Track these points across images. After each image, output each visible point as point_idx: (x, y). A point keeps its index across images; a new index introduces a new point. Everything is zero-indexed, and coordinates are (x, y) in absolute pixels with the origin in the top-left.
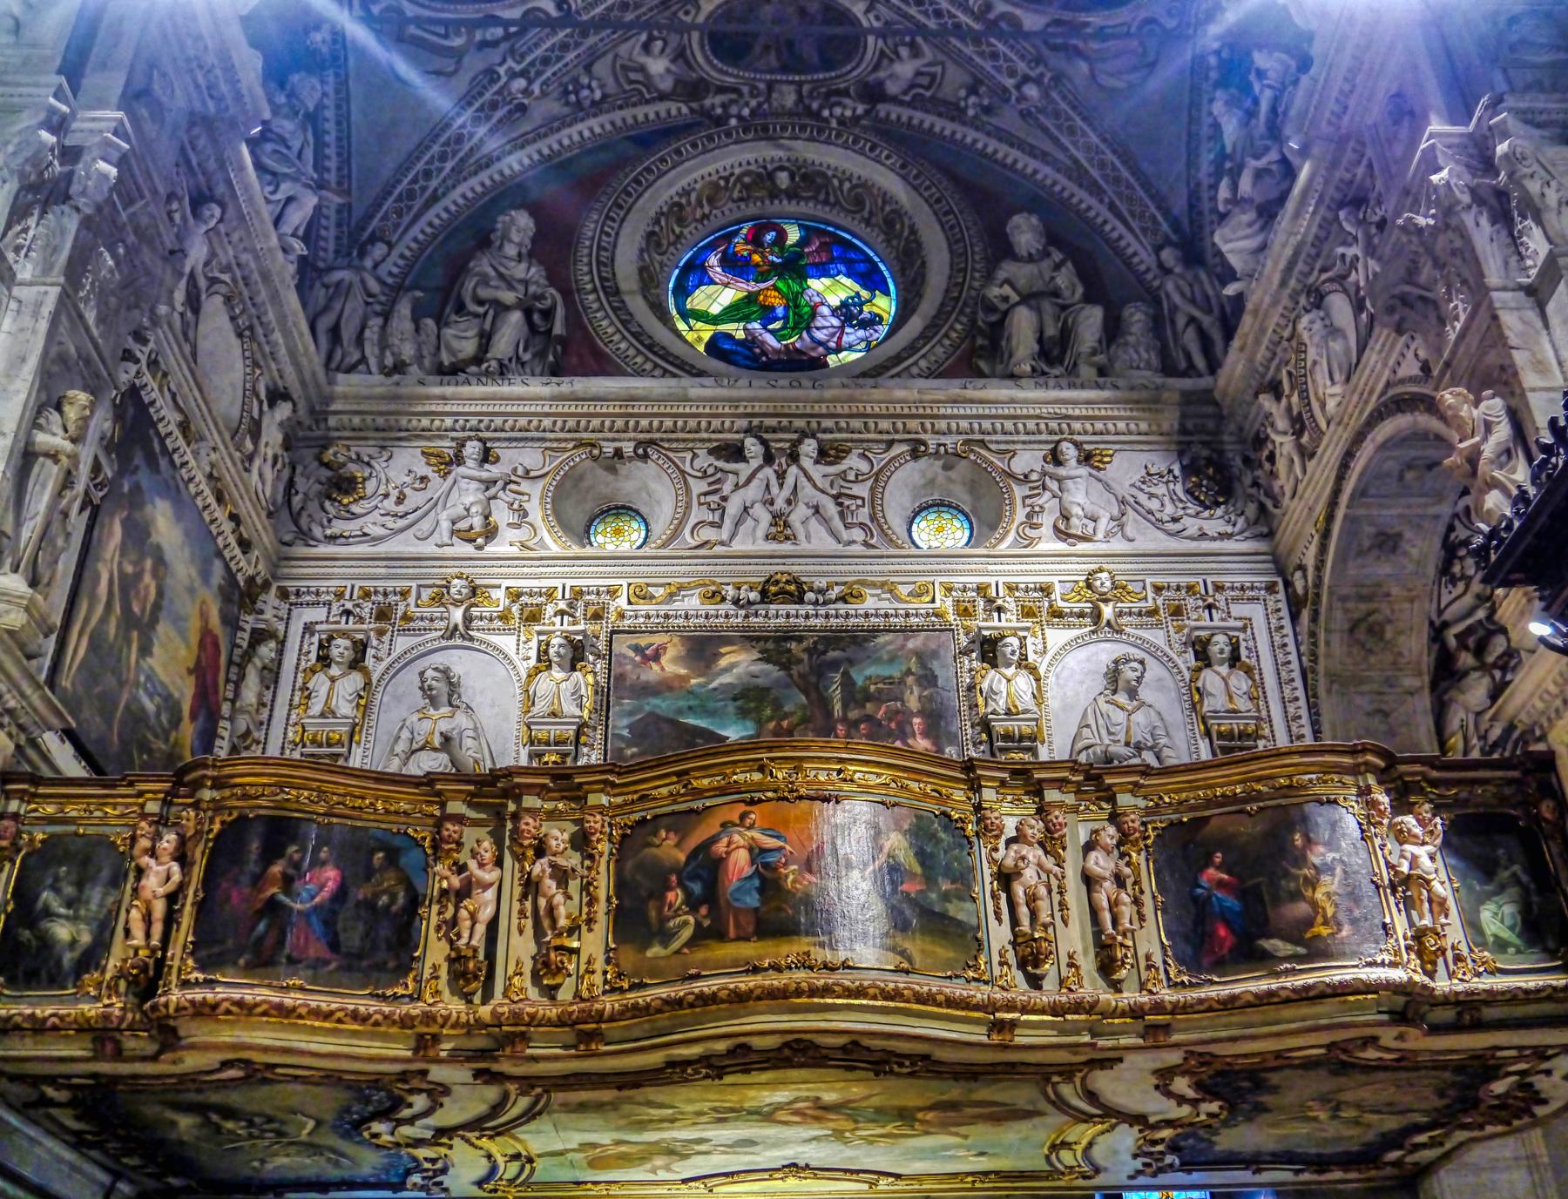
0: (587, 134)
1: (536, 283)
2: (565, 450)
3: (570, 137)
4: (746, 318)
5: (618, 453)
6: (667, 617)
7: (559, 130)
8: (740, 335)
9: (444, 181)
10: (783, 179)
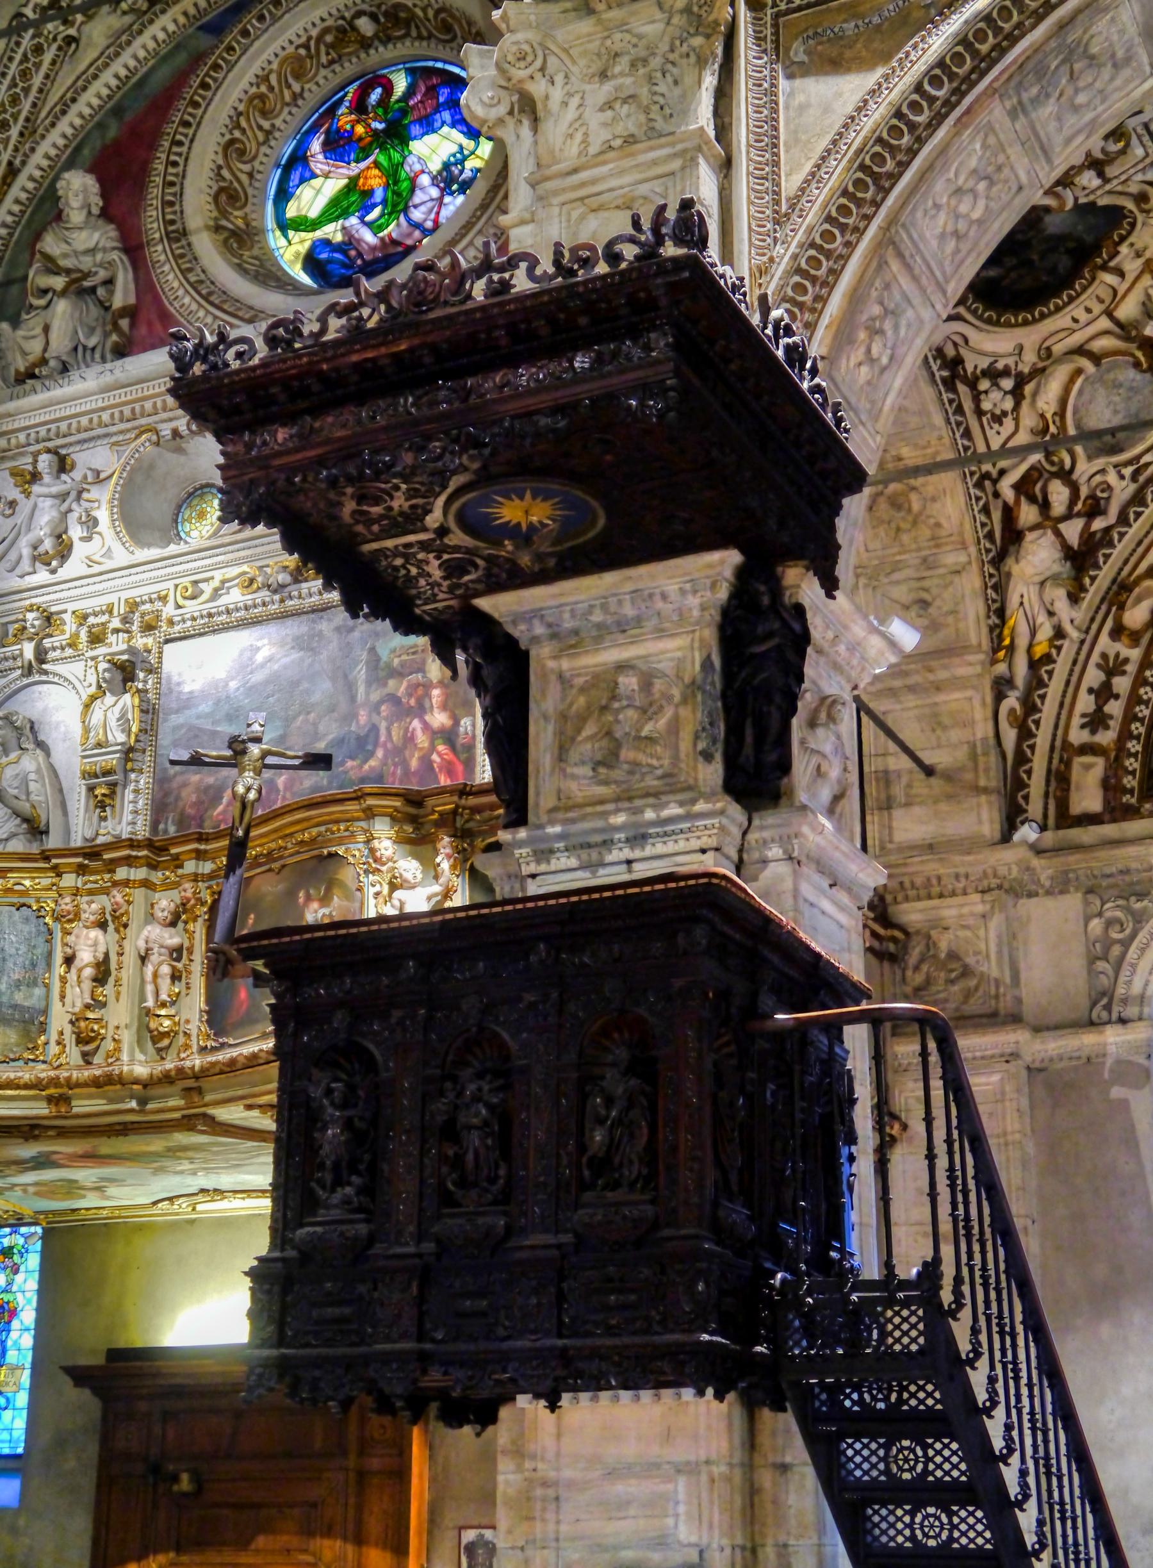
0: (161, 36)
1: (104, 250)
2: (128, 442)
3: (144, 47)
4: (345, 214)
5: (176, 433)
6: (210, 615)
7: (129, 43)
8: (339, 238)
9: (16, 150)
10: (365, 26)
